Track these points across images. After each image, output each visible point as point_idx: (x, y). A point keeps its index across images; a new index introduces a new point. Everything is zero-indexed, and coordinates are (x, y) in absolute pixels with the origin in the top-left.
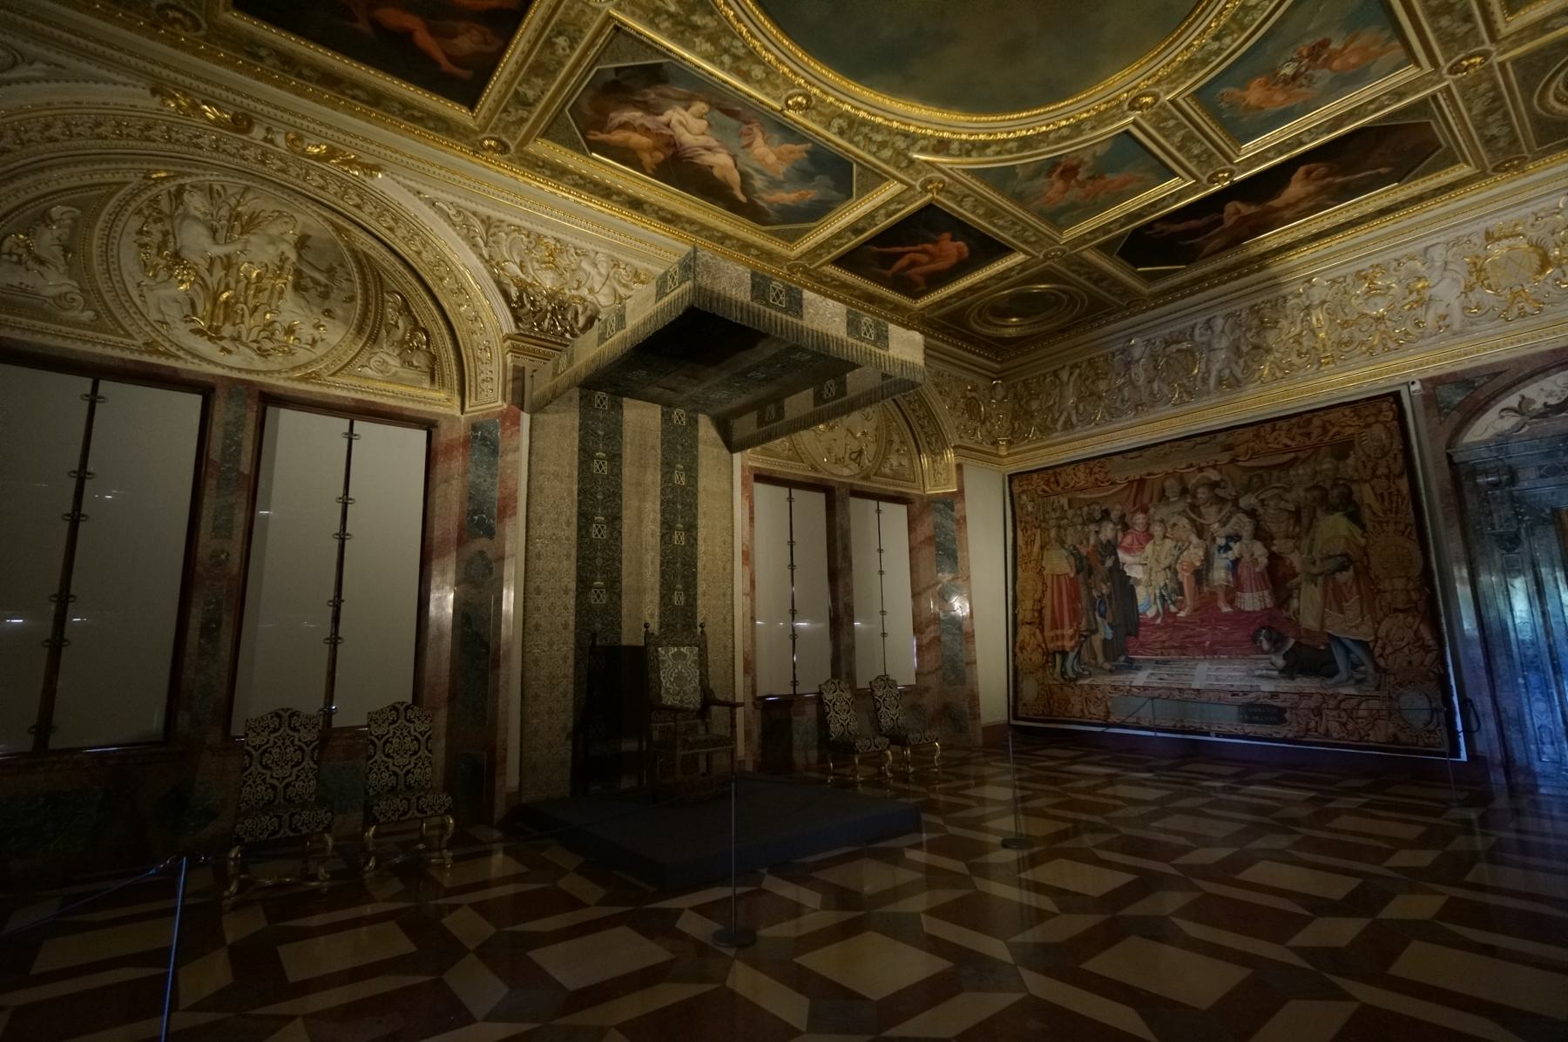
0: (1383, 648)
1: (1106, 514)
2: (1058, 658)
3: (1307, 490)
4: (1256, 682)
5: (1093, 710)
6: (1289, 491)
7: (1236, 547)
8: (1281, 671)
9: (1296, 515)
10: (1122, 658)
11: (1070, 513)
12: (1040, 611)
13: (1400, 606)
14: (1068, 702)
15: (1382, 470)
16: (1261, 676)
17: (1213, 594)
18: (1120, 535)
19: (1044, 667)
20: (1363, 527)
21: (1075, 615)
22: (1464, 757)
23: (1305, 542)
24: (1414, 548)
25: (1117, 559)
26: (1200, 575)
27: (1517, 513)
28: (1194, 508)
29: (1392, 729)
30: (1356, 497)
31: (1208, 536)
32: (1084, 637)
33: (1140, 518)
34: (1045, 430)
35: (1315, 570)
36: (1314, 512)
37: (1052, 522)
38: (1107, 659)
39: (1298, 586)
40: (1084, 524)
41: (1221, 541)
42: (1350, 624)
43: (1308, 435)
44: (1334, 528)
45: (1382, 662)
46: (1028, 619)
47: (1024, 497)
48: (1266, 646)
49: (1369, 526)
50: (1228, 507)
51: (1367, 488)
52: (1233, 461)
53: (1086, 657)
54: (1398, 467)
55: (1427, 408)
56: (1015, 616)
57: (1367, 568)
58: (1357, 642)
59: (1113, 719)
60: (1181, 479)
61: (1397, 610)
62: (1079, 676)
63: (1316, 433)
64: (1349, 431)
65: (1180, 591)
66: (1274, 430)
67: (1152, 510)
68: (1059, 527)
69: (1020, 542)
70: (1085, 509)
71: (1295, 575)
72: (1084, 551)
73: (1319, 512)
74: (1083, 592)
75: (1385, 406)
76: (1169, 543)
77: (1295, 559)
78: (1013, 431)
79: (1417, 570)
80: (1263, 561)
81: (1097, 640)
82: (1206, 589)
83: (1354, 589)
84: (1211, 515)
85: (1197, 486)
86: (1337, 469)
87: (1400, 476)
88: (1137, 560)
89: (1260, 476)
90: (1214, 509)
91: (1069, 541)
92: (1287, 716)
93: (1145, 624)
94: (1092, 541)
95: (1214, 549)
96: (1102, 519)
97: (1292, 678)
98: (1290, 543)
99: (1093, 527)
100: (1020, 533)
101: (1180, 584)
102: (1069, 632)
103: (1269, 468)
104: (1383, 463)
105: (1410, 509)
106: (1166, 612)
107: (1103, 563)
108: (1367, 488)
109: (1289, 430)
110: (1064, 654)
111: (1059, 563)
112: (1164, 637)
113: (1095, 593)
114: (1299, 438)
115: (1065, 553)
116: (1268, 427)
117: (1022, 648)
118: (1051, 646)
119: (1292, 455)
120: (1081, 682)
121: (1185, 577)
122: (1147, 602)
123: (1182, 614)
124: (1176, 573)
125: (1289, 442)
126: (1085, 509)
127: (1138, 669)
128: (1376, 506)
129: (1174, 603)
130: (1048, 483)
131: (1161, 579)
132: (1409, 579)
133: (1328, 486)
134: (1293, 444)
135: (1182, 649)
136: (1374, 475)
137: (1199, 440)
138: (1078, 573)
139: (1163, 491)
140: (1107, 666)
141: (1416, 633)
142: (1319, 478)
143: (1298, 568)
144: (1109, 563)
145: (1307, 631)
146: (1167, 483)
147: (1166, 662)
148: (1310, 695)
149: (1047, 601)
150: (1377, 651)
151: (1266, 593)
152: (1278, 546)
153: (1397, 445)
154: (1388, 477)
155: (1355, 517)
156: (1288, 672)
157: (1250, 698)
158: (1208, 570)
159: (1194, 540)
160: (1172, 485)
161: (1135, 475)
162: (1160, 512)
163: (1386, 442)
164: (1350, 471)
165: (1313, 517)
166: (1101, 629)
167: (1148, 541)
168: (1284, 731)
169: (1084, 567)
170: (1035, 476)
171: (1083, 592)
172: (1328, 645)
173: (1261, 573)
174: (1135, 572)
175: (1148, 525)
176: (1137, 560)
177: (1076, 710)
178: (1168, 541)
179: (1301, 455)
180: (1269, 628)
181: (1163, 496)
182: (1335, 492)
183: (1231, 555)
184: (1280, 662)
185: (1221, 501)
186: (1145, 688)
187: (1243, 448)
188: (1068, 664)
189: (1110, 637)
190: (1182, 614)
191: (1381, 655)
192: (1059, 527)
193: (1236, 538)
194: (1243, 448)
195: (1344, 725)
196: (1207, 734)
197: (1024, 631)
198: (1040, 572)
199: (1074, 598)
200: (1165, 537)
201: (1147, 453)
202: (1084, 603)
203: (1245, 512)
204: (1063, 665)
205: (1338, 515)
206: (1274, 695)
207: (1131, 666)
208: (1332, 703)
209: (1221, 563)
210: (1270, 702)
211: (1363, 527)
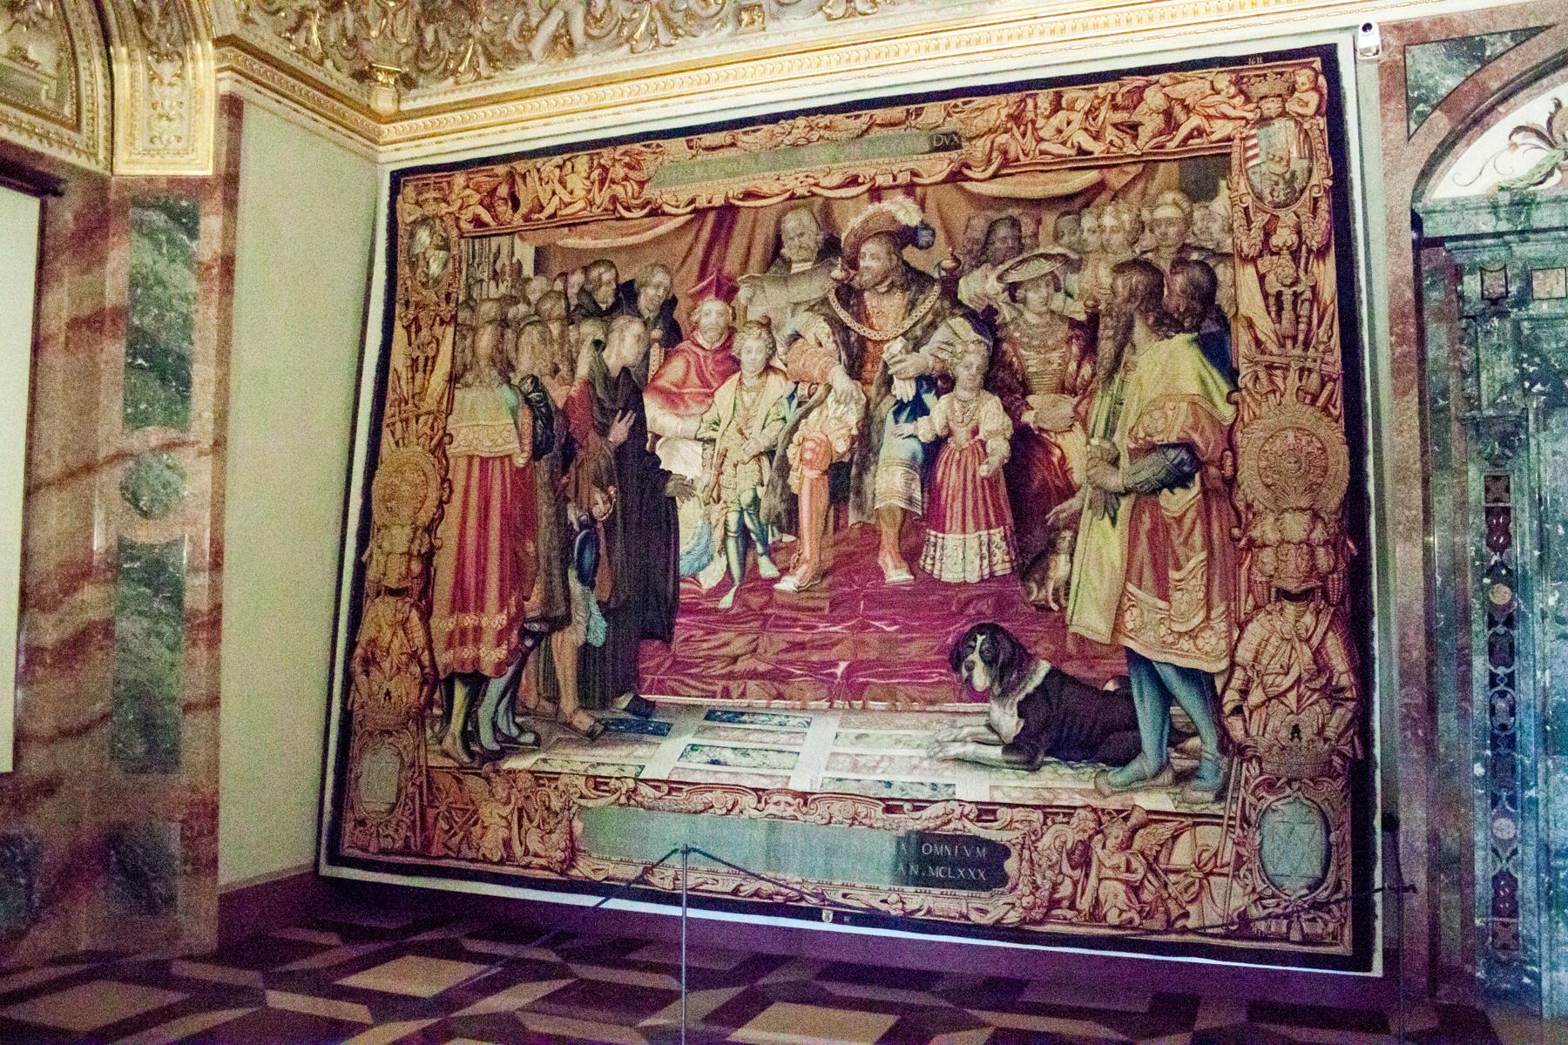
0: (1244, 693)
1: (627, 294)
2: (460, 693)
3: (1119, 269)
4: (948, 775)
5: (534, 844)
6: (1074, 266)
7: (939, 407)
8: (1009, 748)
9: (1087, 331)
10: (624, 701)
11: (537, 286)
12: (428, 558)
13: (1292, 586)
14: (473, 817)
15: (1284, 237)
16: (960, 760)
17: (870, 534)
18: (656, 353)
19: (419, 717)
20: (1231, 375)
21: (516, 576)
22: (1377, 970)
23: (1099, 408)
24: (1334, 436)
25: (640, 423)
26: (844, 479)
27: (1523, 375)
28: (849, 294)
29: (1238, 902)
30: (1222, 297)
31: (874, 372)
32: (533, 636)
33: (711, 312)
34: (501, 55)
35: (1115, 481)
36: (1129, 327)
37: (489, 309)
38: (586, 700)
39: (1073, 522)
40: (569, 319)
41: (904, 390)
42: (1179, 629)
43: (1133, 128)
44: (1167, 370)
45: (1236, 727)
46: (392, 582)
47: (423, 235)
48: (981, 679)
49: (1245, 380)
50: (932, 298)
51: (1248, 275)
52: (956, 177)
53: (530, 693)
54: (1318, 230)
55: (1385, 97)
56: (360, 569)
57: (1231, 482)
58: (1189, 675)
59: (582, 870)
60: (826, 217)
61: (1284, 594)
62: (510, 746)
63: (1152, 125)
64: (1221, 129)
65: (789, 519)
66: (1057, 107)
67: (743, 294)
68: (504, 323)
69: (398, 361)
70: (577, 279)
71: (1069, 491)
72: (559, 394)
73: (1140, 331)
74: (544, 510)
75: (1303, 77)
76: (777, 386)
77: (1074, 449)
78: (421, 53)
79: (1333, 498)
80: (999, 449)
81: (565, 646)
82: (853, 518)
83: (1197, 539)
84: (887, 313)
85: (861, 238)
86: (1188, 221)
87: (1321, 254)
88: (691, 425)
89: (1015, 223)
90: (898, 300)
91: (525, 363)
92: (1010, 865)
93: (691, 610)
94: (583, 370)
95: (886, 409)
96: (615, 309)
97: (1032, 766)
98: (1067, 405)
99: (590, 329)
100: (399, 333)
101: (793, 500)
102: (494, 620)
103: (1037, 203)
104: (1287, 216)
105: (1335, 341)
106: (750, 572)
107: (604, 431)
108: (1248, 275)
109: (1091, 112)
110: (477, 683)
111: (489, 424)
112: (738, 645)
113: (573, 515)
114: (1111, 134)
115: (508, 396)
116: (1044, 98)
117: (369, 662)
118: (444, 658)
119: (1092, 177)
120: (512, 763)
121: (807, 482)
122: (703, 551)
123: (788, 584)
124: (784, 469)
125: (1088, 143)
126: (577, 279)
127: (662, 731)
128: (1265, 326)
129: (771, 552)
130: (489, 201)
131: (745, 482)
132: (1316, 516)
133: (1165, 266)
134: (1097, 148)
135: (777, 679)
136: (1266, 248)
137: (880, 114)
138: (536, 454)
139: (778, 243)
140: (584, 721)
141: (1317, 652)
142: (1148, 240)
143: (1077, 477)
144: (620, 431)
145: (1081, 640)
146: (791, 223)
147: (735, 716)
148: (1068, 812)
149: (448, 532)
150: (1231, 698)
151: (997, 534)
152: (1043, 409)
153: (1321, 177)
154: (1295, 255)
155: (1216, 350)
156: (1026, 751)
157: (926, 820)
158: (863, 468)
159: (840, 379)
160: (801, 230)
161: (714, 192)
162: (761, 299)
163: (1299, 166)
164: (1215, 228)
165: (1125, 338)
166: (579, 616)
167: (725, 376)
168: (997, 908)
169: (554, 438)
170: (460, 179)
171: (544, 510)
172: (1124, 681)
173: (991, 482)
174: (682, 460)
175: (731, 332)
176: (691, 425)
177: (491, 845)
178: (773, 379)
179: (1116, 179)
180: (993, 631)
181: (775, 254)
182: (1179, 281)
183: (925, 429)
184: (1009, 721)
185: (915, 280)
186: (674, 786)
187: (980, 147)
188: (484, 713)
189: (598, 638)
190: (788, 584)
191: (1238, 710)
192: (504, 323)
193: (939, 382)
194: (980, 147)
195: (1135, 889)
196: (814, 914)
197: (380, 612)
198: (439, 449)
199: (519, 526)
200: (768, 368)
201: (747, 139)
202: (542, 543)
203: (970, 315)
204: (471, 714)
205: (1181, 339)
206: (986, 811)
207: (646, 723)
208: (1117, 832)
209: (899, 445)
210: (975, 829)
211: (1231, 375)
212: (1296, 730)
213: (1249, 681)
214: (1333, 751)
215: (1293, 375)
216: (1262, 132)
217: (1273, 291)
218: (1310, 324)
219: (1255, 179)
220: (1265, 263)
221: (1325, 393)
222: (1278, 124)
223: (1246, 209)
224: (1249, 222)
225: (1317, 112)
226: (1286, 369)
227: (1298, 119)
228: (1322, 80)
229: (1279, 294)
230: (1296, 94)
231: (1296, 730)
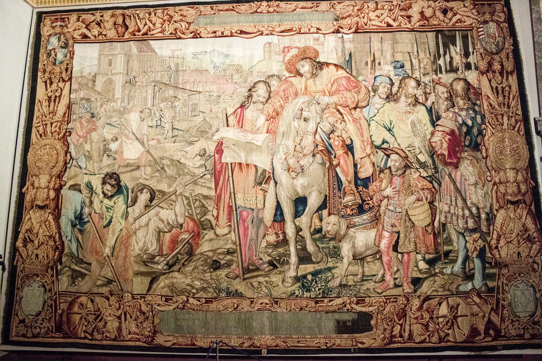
54: (509, 66)
87: (511, 73)
105: (519, 107)
154: (501, 74)
212: (519, 254)
214: (534, 262)
215: (505, 118)
216: (485, 26)
218: (509, 99)
220: (490, 75)
221: (518, 126)
222: (491, 24)
225: (504, 22)
226: (502, 115)
227: (497, 22)
228: (505, 9)
229: (497, 87)
230: (496, 13)
231: (519, 254)
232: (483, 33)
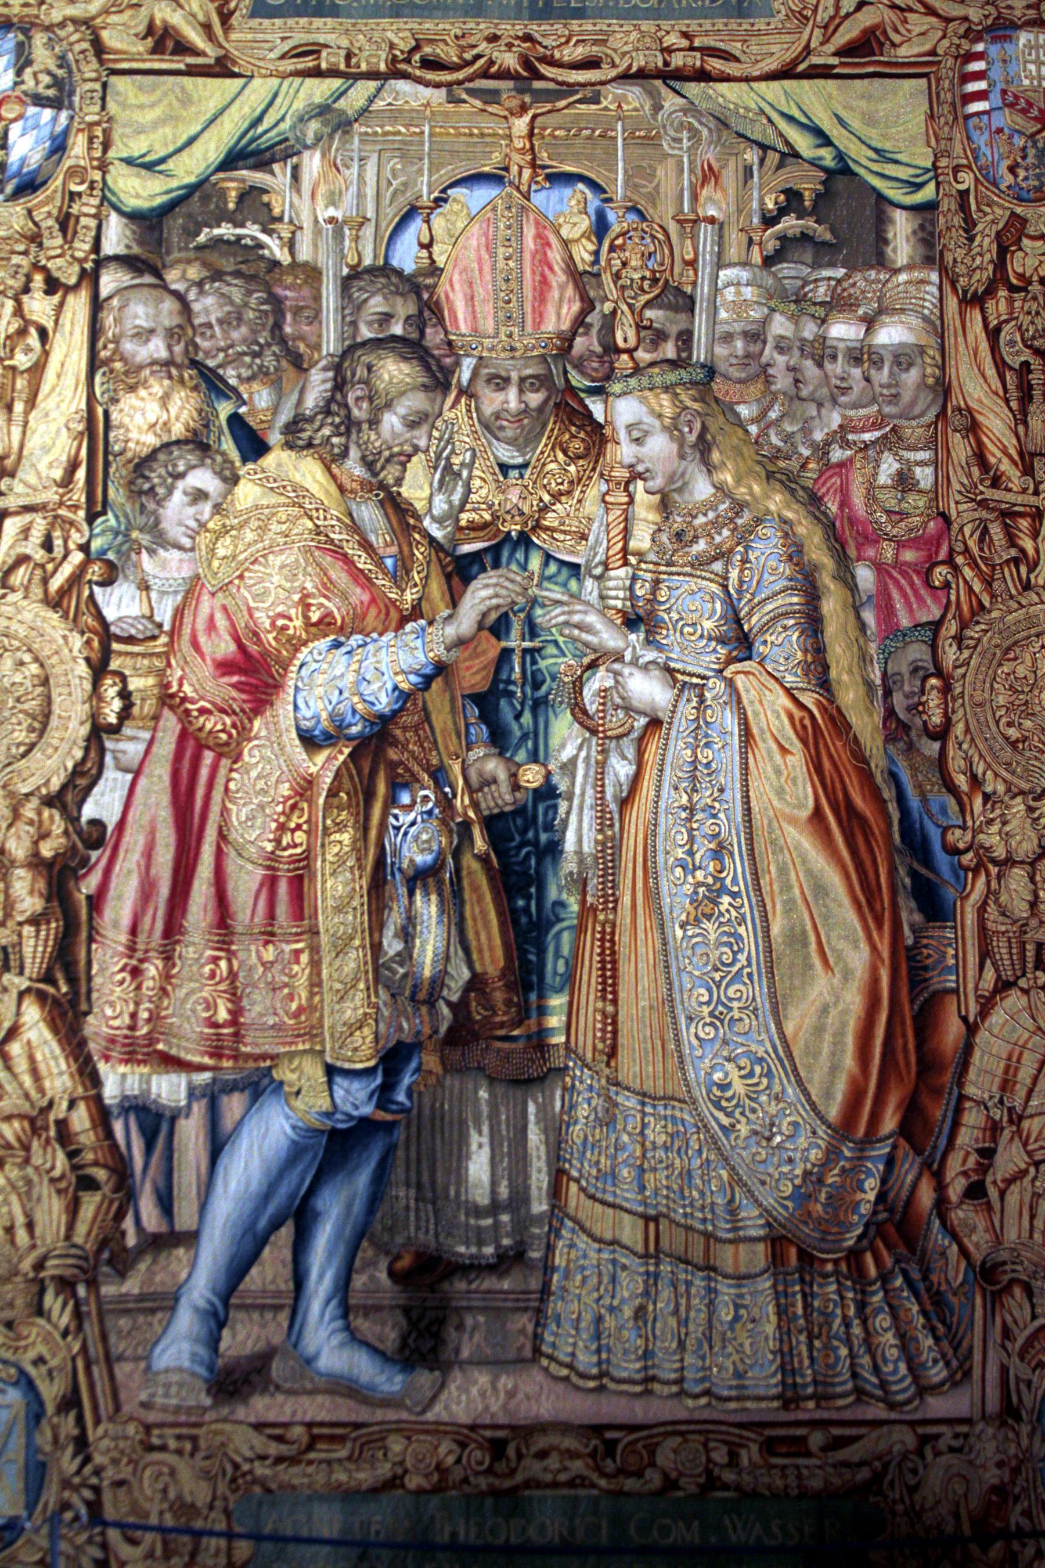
213: (994, 1129)
216: (994, 50)
217: (1015, 362)
219: (981, 140)
220: (998, 306)
223: (964, 194)
224: (970, 225)
232: (982, 85)
